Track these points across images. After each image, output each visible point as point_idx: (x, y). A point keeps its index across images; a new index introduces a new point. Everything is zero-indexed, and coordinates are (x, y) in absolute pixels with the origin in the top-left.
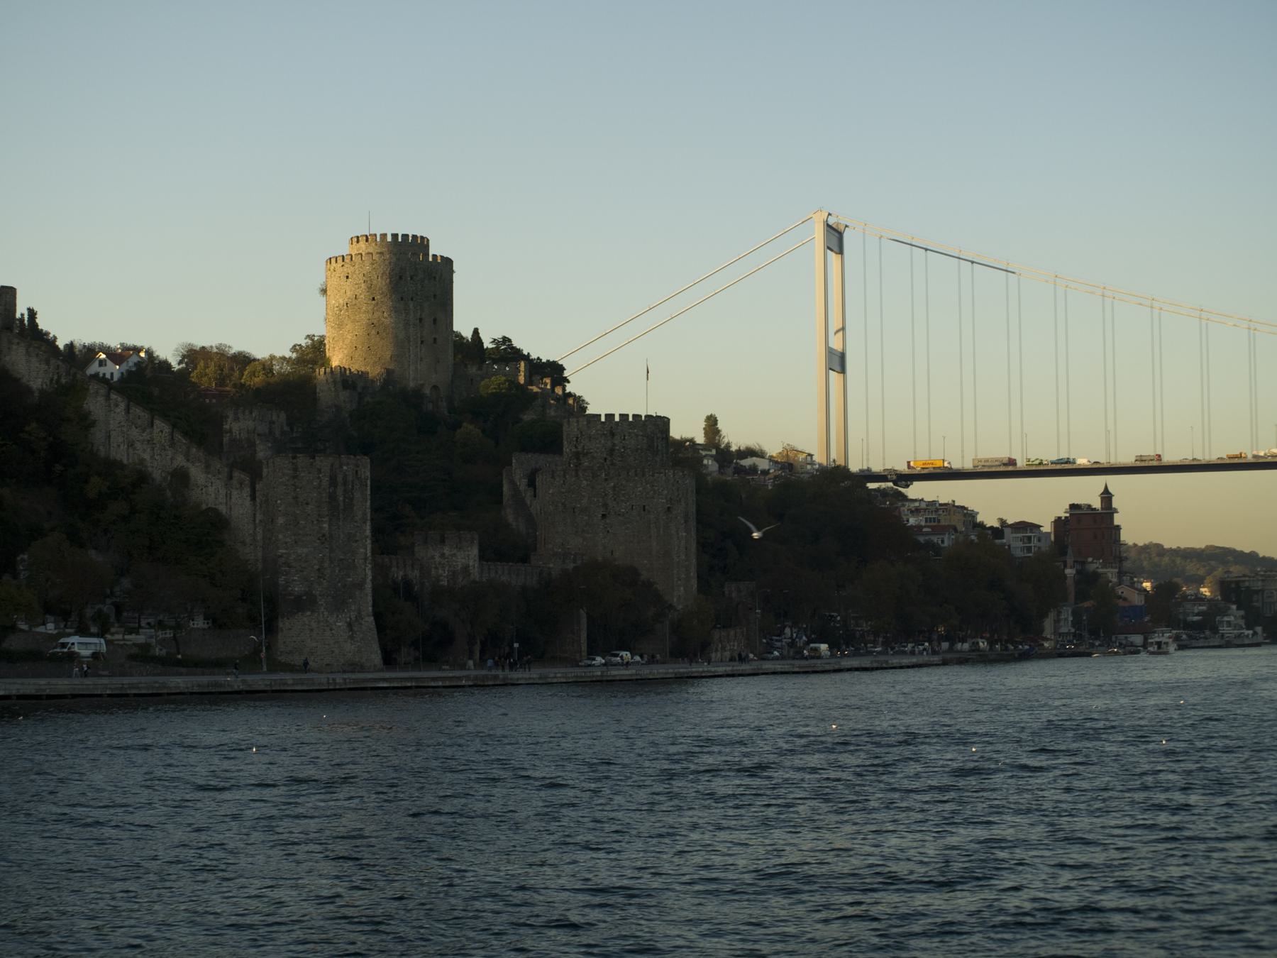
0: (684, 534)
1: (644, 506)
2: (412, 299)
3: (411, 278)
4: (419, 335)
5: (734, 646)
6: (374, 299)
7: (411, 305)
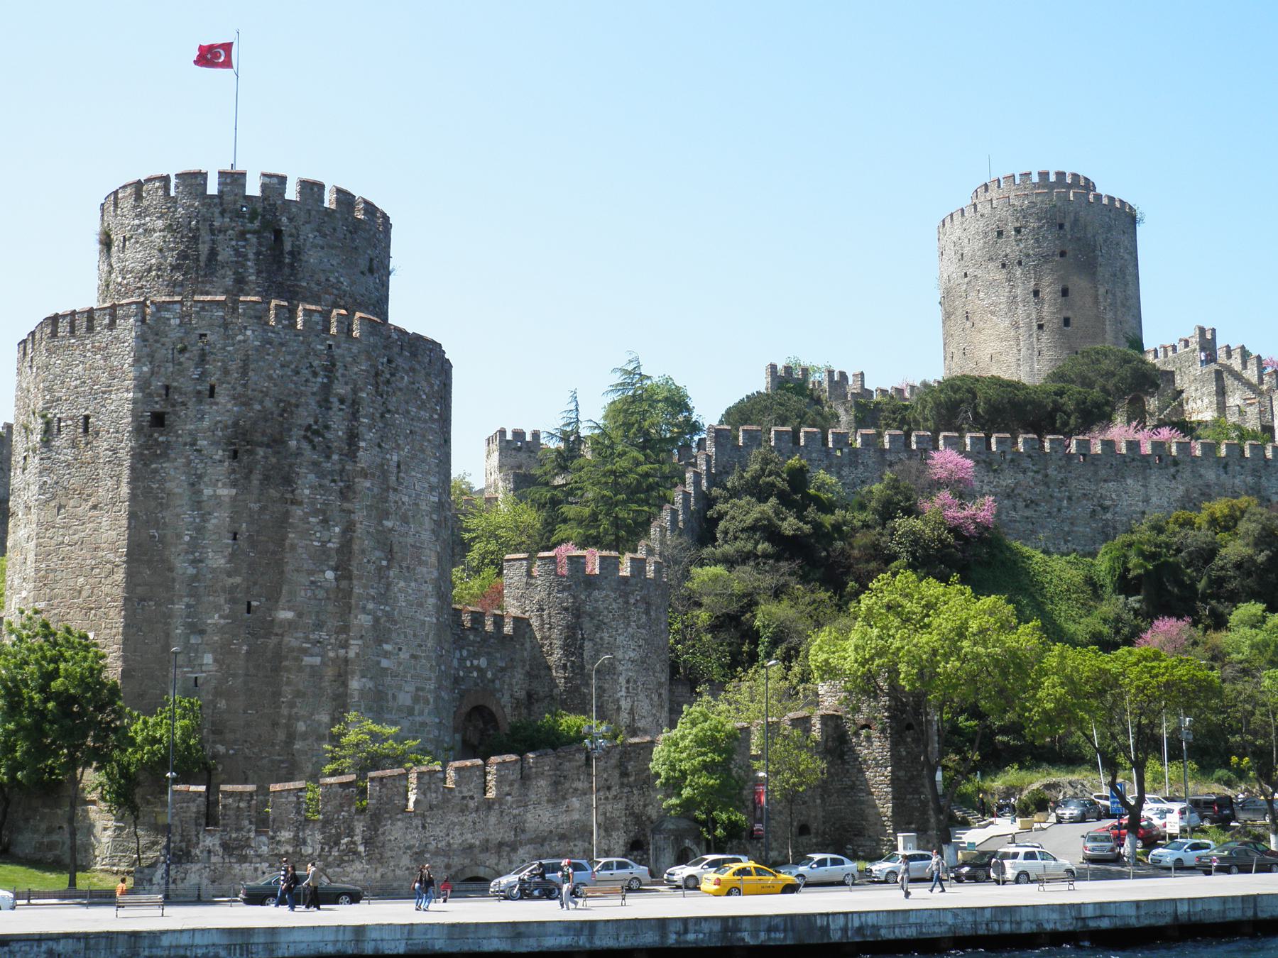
0: (224, 492)
1: (87, 418)
2: (1020, 263)
3: (1018, 231)
5: (299, 842)
6: (966, 275)
7: (1018, 272)
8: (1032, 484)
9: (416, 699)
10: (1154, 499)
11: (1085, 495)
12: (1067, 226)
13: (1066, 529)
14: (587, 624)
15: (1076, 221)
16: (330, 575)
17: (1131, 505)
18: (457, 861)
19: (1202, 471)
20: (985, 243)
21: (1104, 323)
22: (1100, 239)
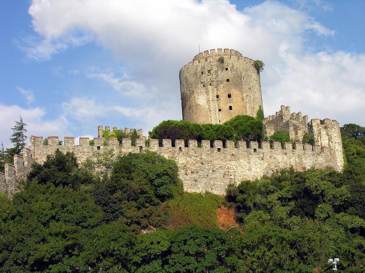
2: (210, 84)
3: (209, 71)
4: (217, 106)
7: (210, 88)
8: (194, 162)
10: (253, 169)
11: (221, 167)
13: (212, 183)
15: (233, 67)
17: (243, 172)
19: (275, 156)
20: (196, 77)
21: (246, 108)
22: (243, 74)
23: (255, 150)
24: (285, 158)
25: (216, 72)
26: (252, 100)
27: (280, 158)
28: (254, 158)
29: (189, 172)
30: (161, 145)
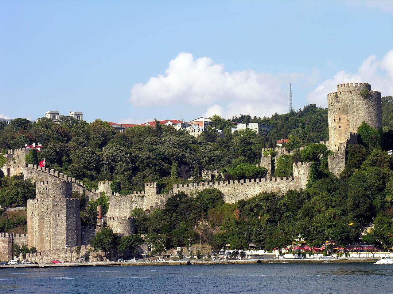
9: (62, 242)
10: (256, 191)
12: (340, 102)
14: (113, 226)
16: (49, 229)
18: (52, 260)
22: (349, 104)
23: (258, 183)
24: (271, 185)
25: (334, 103)
26: (355, 120)
27: (269, 185)
28: (257, 186)
29: (229, 194)
30: (219, 184)
